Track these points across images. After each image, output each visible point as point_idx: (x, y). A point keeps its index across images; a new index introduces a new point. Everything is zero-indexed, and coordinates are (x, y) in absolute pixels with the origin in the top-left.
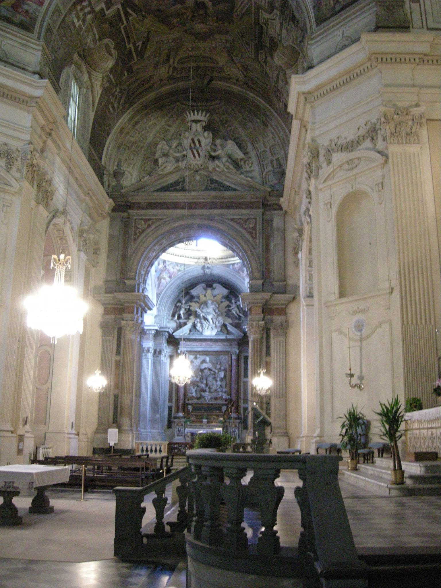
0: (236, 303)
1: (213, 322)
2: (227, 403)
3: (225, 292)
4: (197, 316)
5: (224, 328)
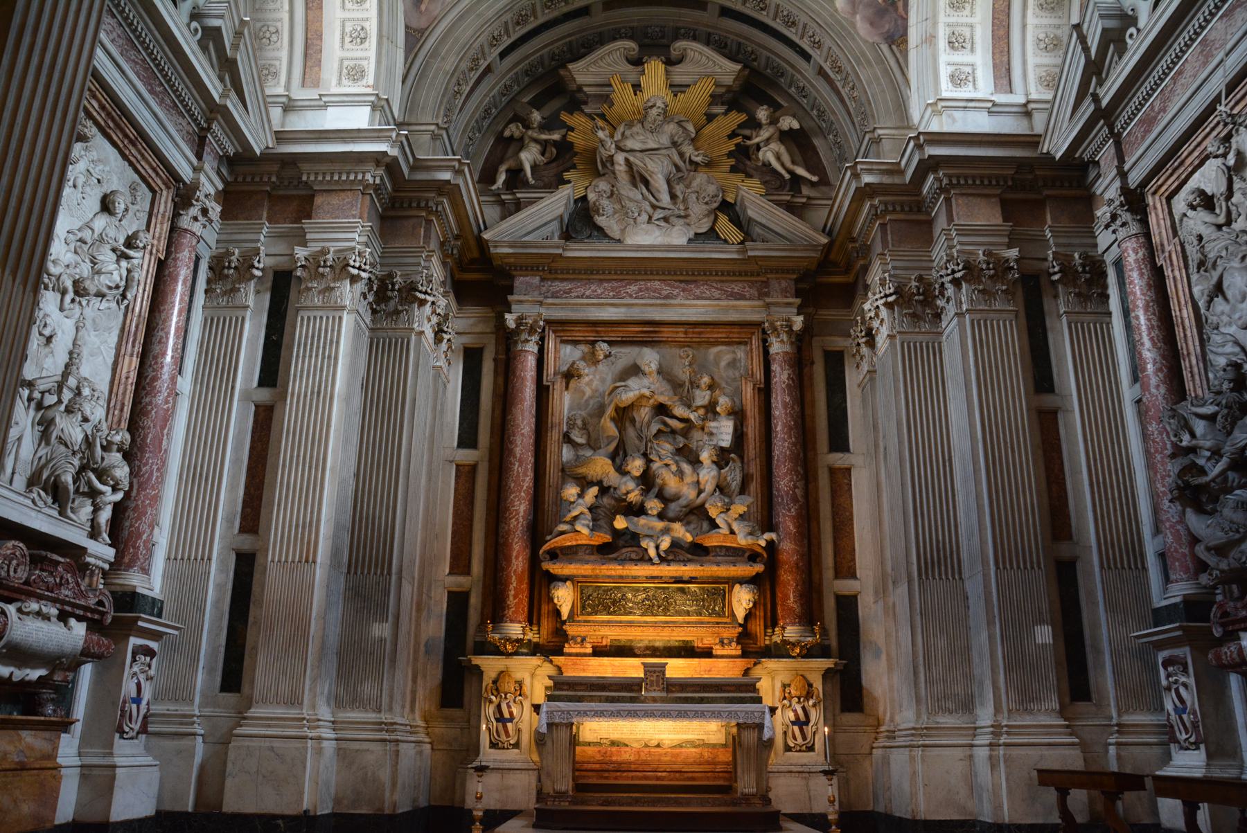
0: (773, 121)
1: (673, 197)
2: (759, 568)
3: (728, 70)
4: (597, 166)
5: (723, 220)
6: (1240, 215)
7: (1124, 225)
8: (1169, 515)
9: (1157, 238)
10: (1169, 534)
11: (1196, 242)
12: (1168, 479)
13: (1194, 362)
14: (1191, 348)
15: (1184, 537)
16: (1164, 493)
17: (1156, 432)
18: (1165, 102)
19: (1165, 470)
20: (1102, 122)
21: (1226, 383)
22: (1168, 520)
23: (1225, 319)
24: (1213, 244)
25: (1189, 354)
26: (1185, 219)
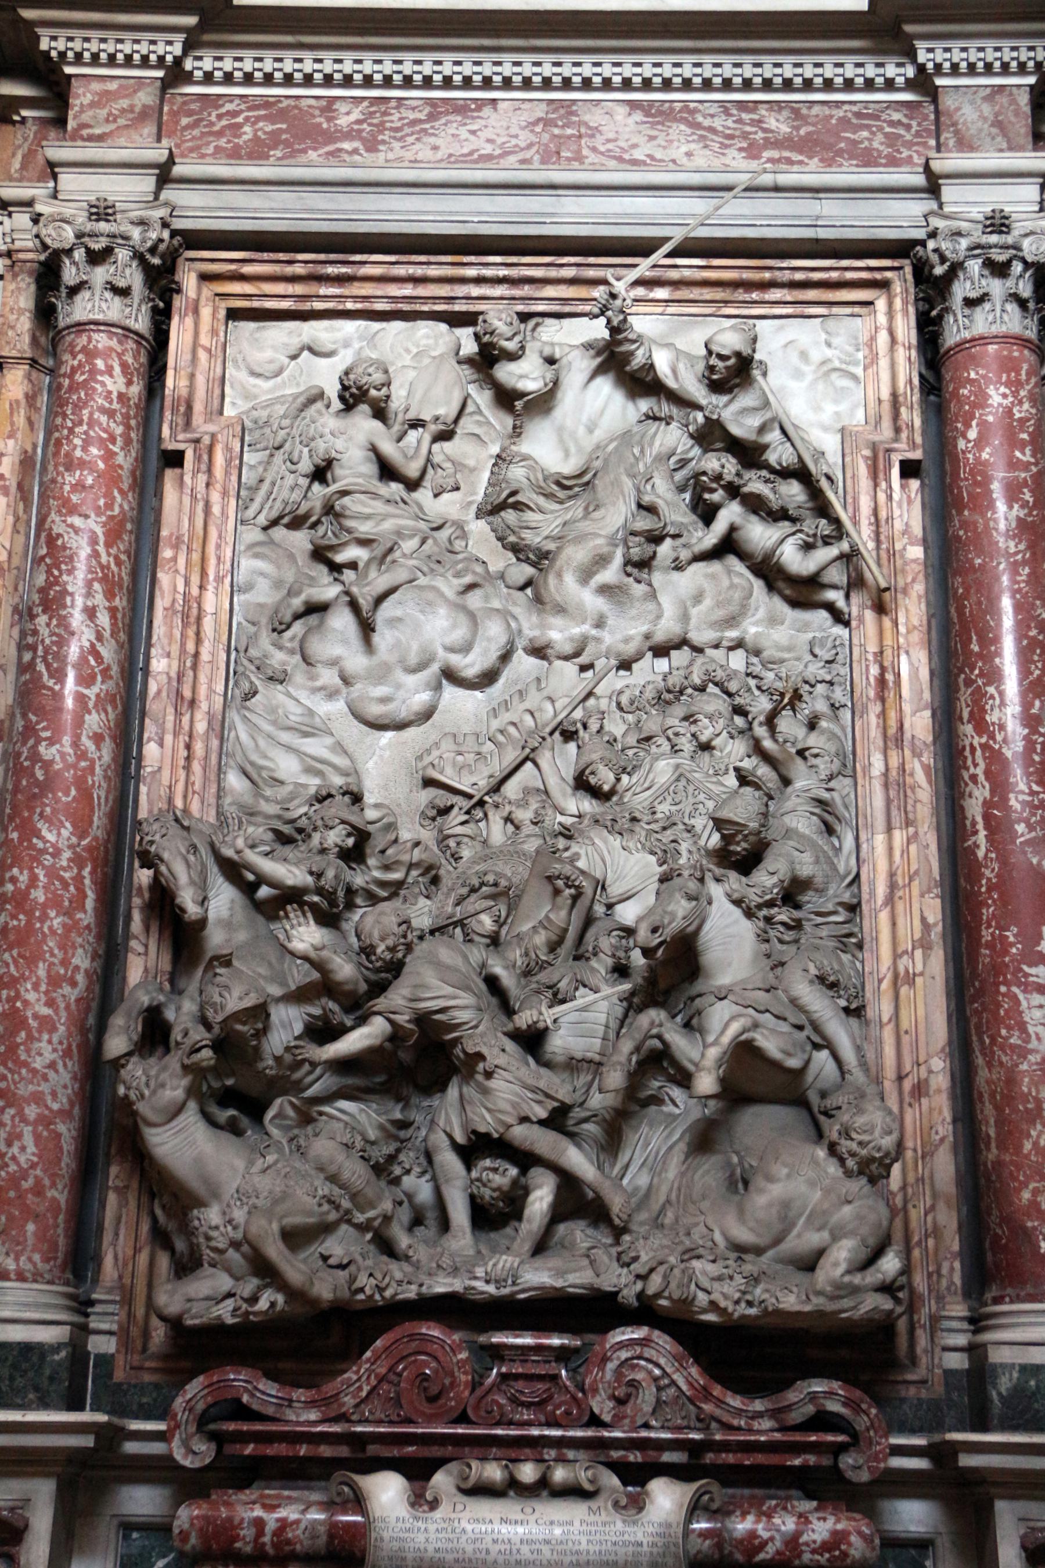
6: (458, 489)
7: (123, 292)
8: (44, 1087)
9: (183, 383)
10: (28, 1140)
11: (306, 466)
12: (67, 989)
13: (201, 727)
14: (203, 691)
15: (66, 1160)
16: (47, 1024)
17: (67, 854)
18: (381, 127)
19: (65, 963)
20: (191, 20)
21: (341, 830)
22: (37, 1098)
23: (328, 677)
24: (379, 506)
25: (193, 703)
26: (319, 405)
